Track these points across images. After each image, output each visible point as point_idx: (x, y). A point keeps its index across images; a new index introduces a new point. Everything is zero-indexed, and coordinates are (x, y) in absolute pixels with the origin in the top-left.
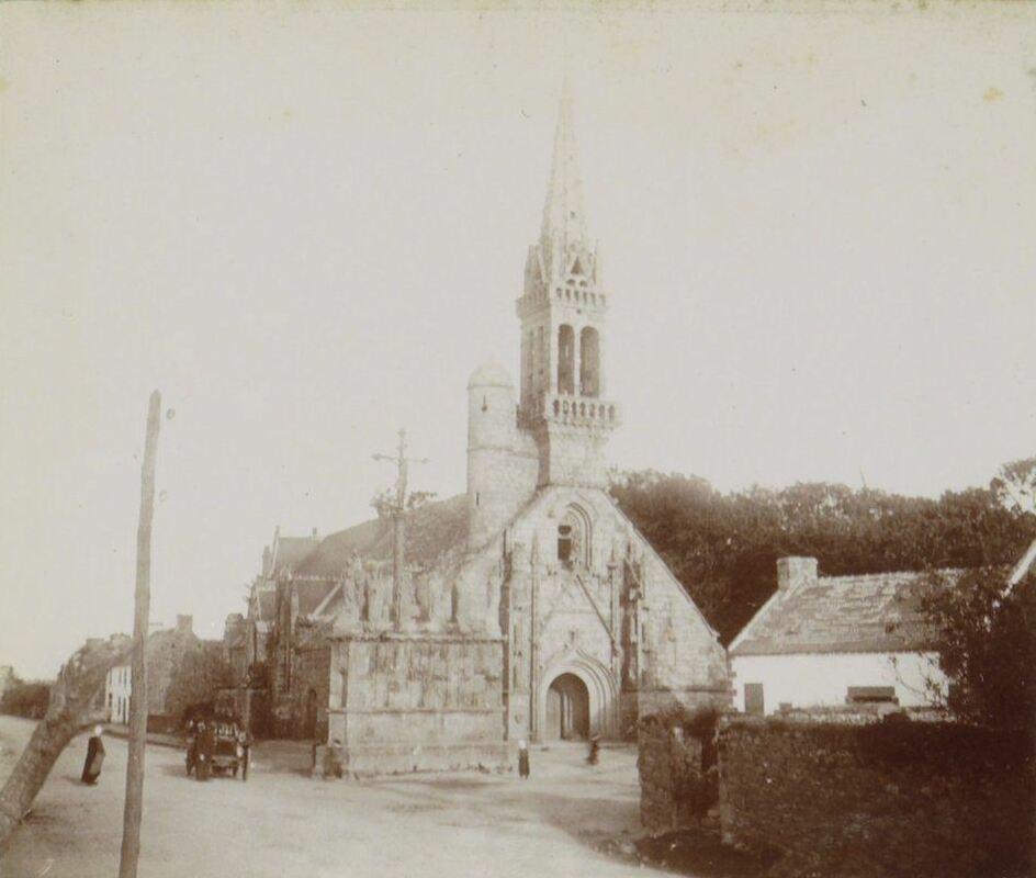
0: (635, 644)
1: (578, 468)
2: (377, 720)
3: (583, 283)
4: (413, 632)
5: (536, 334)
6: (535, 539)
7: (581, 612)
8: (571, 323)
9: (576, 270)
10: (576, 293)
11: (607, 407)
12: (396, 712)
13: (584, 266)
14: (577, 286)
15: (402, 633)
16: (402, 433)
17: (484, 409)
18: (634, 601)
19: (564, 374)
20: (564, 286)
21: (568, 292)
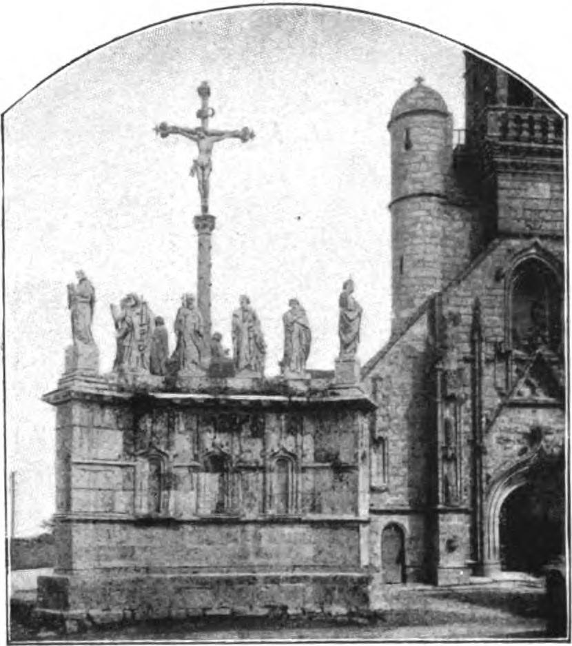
16: (204, 92)
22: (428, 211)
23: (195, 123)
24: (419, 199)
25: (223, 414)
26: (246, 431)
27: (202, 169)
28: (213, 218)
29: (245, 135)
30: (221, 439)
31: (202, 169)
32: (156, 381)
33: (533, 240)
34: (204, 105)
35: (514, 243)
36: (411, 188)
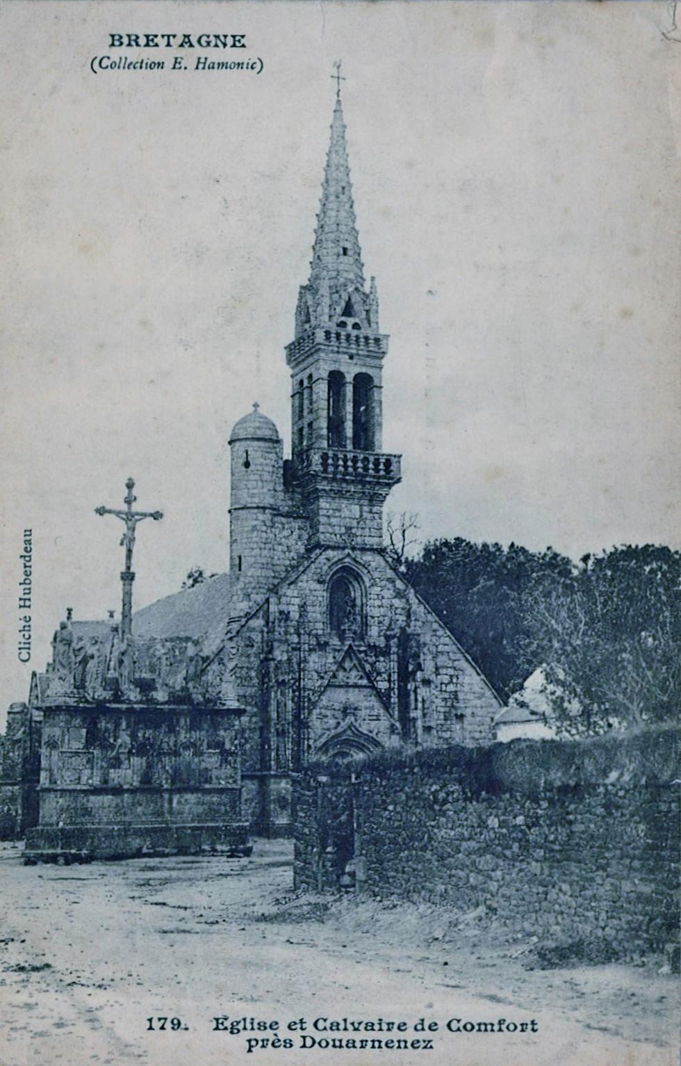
0: (415, 719)
1: (351, 528)
2: (95, 801)
3: (356, 326)
4: (137, 703)
5: (306, 383)
6: (303, 607)
7: (355, 686)
8: (343, 369)
9: (348, 311)
10: (348, 336)
11: (383, 460)
12: (118, 791)
13: (358, 307)
14: (349, 328)
15: (123, 702)
16: (130, 486)
17: (247, 464)
18: (414, 673)
19: (335, 425)
20: (334, 329)
21: (338, 335)
22: (264, 521)
23: (124, 507)
24: (256, 511)
25: (150, 716)
26: (164, 728)
27: (128, 542)
28: (134, 574)
29: (157, 516)
30: (149, 733)
31: (128, 542)
32: (107, 695)
33: (347, 551)
34: (130, 493)
35: (330, 553)
36: (245, 499)
